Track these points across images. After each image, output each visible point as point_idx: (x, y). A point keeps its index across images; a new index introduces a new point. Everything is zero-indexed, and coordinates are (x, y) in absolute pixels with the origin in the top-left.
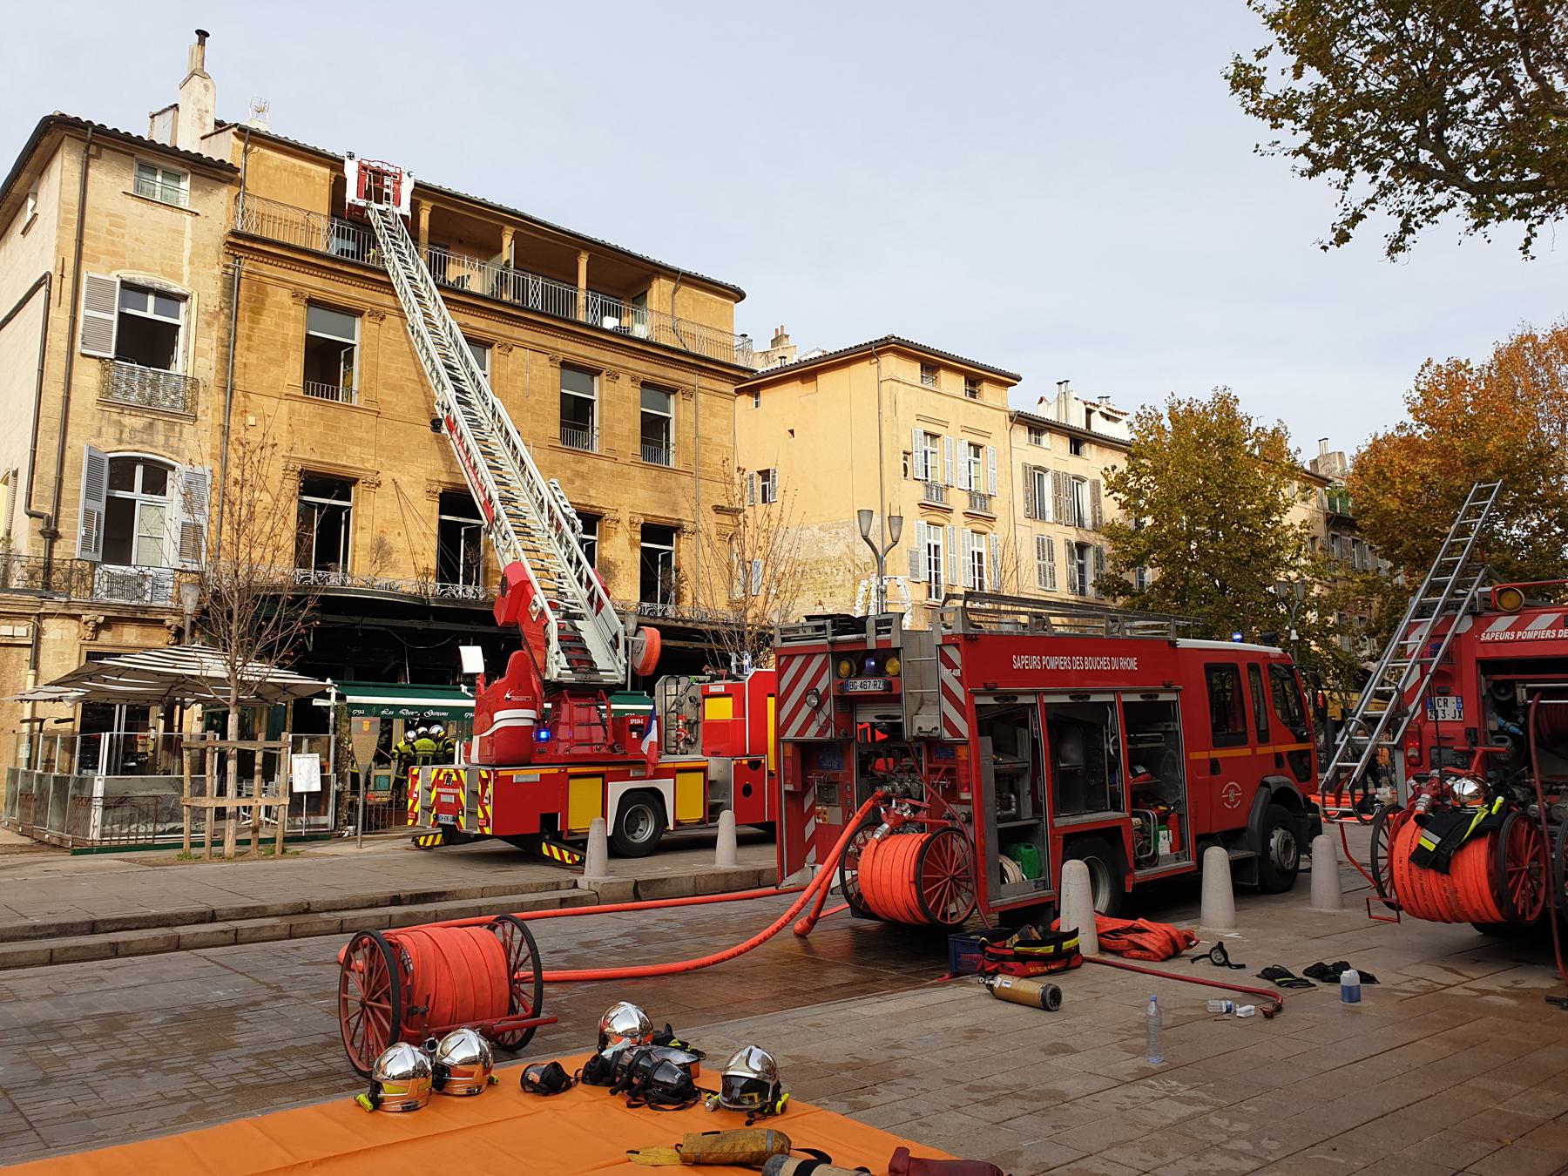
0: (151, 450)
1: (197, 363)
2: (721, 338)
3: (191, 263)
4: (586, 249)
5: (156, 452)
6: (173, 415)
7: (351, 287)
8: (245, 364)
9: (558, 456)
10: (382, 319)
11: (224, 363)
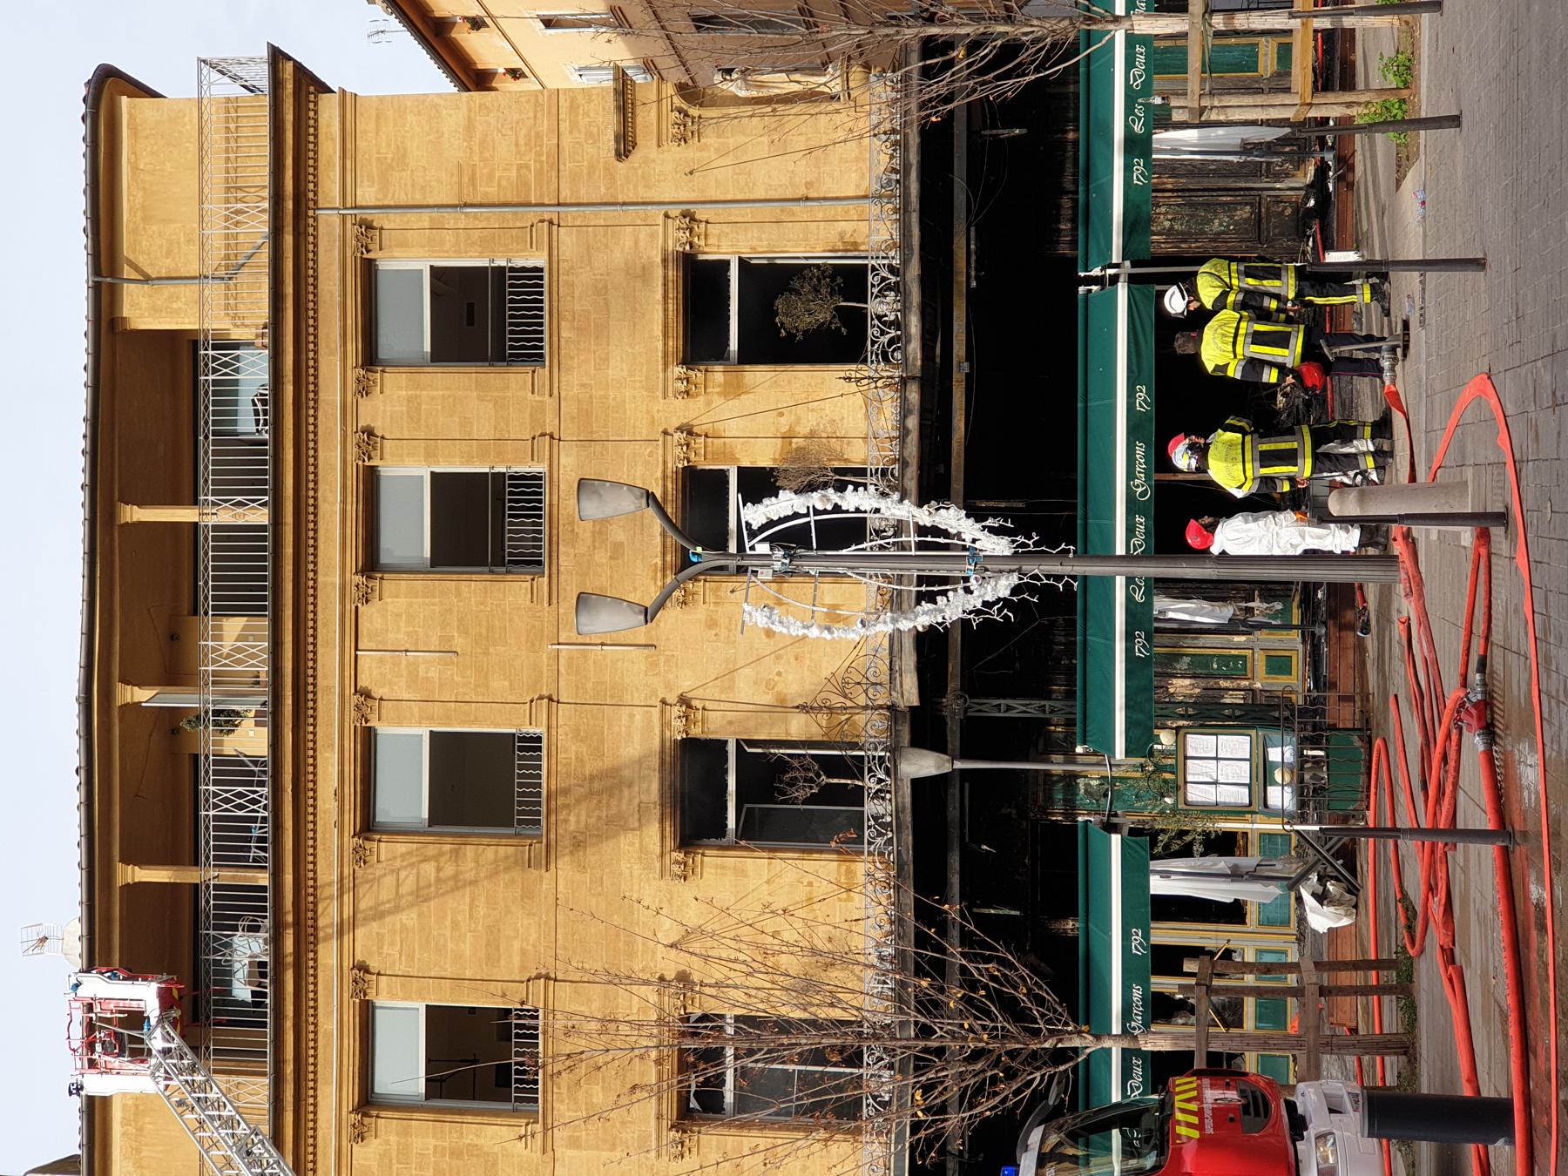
7: (321, 1030)
10: (367, 971)
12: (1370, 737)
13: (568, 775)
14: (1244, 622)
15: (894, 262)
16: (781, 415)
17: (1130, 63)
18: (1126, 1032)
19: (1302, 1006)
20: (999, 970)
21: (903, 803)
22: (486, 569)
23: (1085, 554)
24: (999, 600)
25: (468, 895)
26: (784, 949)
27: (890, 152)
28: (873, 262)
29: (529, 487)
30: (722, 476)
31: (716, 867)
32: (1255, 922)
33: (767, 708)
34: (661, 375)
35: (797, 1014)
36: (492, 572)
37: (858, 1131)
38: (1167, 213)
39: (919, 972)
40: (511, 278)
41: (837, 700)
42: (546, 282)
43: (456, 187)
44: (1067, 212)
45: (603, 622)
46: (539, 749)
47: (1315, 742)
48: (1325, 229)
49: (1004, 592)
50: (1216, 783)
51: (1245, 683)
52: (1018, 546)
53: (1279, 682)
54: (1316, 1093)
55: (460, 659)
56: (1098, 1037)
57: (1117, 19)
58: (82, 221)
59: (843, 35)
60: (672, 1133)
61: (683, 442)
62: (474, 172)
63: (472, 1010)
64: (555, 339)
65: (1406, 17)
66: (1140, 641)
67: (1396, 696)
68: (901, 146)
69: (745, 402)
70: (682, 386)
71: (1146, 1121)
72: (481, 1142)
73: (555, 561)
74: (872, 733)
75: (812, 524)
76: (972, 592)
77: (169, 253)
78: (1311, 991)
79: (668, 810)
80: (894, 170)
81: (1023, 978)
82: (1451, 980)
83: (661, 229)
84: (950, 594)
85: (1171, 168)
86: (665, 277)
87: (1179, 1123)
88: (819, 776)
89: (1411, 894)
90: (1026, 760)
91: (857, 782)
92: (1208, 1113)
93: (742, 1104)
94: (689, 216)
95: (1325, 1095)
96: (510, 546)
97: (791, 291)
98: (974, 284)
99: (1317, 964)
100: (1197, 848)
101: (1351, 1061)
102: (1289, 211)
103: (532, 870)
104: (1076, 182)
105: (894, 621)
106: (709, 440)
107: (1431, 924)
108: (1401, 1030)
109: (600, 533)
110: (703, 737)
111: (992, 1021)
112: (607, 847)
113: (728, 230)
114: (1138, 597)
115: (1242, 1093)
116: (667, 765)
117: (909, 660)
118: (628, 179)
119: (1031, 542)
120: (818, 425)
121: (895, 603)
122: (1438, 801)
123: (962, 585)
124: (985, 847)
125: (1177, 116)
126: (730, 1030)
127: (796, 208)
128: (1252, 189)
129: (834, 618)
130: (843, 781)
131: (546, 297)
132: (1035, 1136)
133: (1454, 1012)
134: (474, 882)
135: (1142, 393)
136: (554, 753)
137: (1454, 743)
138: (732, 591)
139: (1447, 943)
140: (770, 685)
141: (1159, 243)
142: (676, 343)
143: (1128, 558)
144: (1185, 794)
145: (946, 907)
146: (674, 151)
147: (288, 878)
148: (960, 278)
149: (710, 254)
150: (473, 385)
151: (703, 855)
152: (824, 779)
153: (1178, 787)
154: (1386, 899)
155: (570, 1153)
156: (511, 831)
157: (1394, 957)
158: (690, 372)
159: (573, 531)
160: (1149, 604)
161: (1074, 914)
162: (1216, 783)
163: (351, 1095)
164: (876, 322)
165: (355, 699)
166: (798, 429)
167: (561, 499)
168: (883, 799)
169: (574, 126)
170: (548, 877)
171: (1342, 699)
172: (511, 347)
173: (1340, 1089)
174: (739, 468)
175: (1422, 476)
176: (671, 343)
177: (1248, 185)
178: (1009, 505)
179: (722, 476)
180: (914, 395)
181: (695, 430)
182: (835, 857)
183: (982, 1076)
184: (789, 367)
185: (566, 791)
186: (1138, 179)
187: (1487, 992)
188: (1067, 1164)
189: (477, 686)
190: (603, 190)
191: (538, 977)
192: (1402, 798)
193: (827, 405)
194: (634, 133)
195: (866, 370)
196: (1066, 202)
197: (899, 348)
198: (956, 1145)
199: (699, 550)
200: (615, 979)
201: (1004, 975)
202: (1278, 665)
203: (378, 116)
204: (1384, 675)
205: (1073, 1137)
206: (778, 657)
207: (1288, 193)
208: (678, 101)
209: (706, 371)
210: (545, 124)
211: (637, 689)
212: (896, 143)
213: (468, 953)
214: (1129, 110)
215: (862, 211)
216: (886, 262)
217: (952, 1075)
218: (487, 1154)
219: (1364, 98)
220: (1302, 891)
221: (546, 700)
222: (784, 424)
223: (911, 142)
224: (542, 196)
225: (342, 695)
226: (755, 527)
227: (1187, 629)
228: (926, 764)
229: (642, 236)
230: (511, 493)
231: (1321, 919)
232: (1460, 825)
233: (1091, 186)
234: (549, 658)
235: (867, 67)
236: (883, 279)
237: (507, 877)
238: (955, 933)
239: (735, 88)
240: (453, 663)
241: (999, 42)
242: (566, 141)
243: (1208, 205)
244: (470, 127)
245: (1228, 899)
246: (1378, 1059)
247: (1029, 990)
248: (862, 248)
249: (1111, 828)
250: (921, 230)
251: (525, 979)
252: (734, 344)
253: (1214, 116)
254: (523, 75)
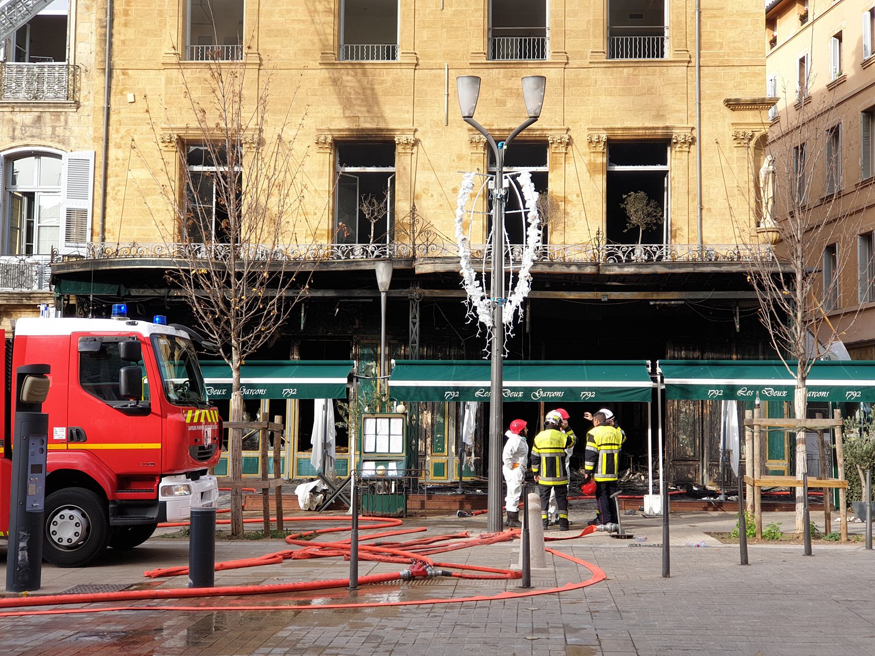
0: (39, 142)
1: (78, 50)
5: (43, 143)
6: (56, 105)
8: (123, 42)
11: (103, 46)
12: (402, 517)
13: (374, 75)
14: (463, 450)
15: (664, 258)
16: (578, 196)
17: (777, 388)
18: (241, 386)
19: (257, 480)
20: (273, 315)
21: (361, 265)
22: (490, 26)
23: (503, 365)
24: (478, 316)
25: (306, 18)
26: (282, 197)
27: (728, 255)
28: (664, 247)
29: (540, 52)
30: (543, 163)
31: (324, 161)
32: (299, 457)
33: (413, 189)
34: (601, 127)
35: (244, 209)
36: (489, 30)
37: (182, 239)
38: (690, 409)
39: (271, 274)
40: (658, 39)
41: (418, 228)
42: (655, 59)
43: (710, 7)
44: (691, 355)
45: (464, 91)
46: (388, 59)
47: (399, 487)
48: (681, 495)
49: (481, 319)
50: (376, 434)
51: (429, 451)
52: (507, 326)
53: (430, 467)
54: (211, 486)
55: (439, 12)
56: (238, 369)
57: (804, 379)
59: (796, 227)
60: (176, 137)
61: (563, 140)
62: (719, 17)
63: (241, 23)
64: (623, 65)
65: (801, 537)
66: (454, 394)
67: (426, 530)
68: (731, 262)
69: (585, 175)
70: (595, 139)
71: (193, 395)
72: (168, 27)
73: (495, 66)
74: (400, 248)
75: (519, 211)
76: (481, 300)
78: (265, 485)
79: (355, 133)
80: (717, 258)
81: (269, 328)
82: (275, 557)
83: (685, 125)
84: (481, 288)
85: (716, 412)
86: (658, 128)
87: (194, 412)
88: (375, 218)
89: (318, 538)
90: (386, 333)
91: (372, 240)
92: (199, 428)
93: (195, 175)
94: (693, 142)
95: (210, 491)
96: (503, 40)
97: (649, 200)
98: (652, 303)
99: (280, 487)
100: (340, 425)
101: (228, 507)
102: (690, 476)
103: (320, 55)
104: (708, 359)
105: (466, 257)
106: (564, 155)
107: (304, 548)
108: (245, 532)
109: (511, 93)
110: (396, 153)
111: (246, 312)
112: (334, 98)
113: (684, 164)
114: (478, 394)
115: (210, 446)
116: (380, 133)
117: (440, 268)
118: (715, 108)
119: (510, 333)
120: (572, 217)
121: (474, 260)
122: (370, 551)
123: (485, 294)
124: (337, 310)
125: (748, 413)
126: (236, 169)
127: (697, 203)
128: (703, 457)
129: (465, 226)
130: (372, 232)
131: (647, 59)
132: (184, 334)
133: (257, 558)
134: (313, 21)
135: (590, 395)
136: (386, 67)
137: (403, 559)
138: (478, 169)
139: (294, 555)
140: (426, 191)
141: (673, 405)
142: (619, 135)
143: (501, 388)
144: (370, 418)
145: (307, 286)
146: (730, 132)
148: (655, 296)
150: (596, 18)
151: (330, 153)
152: (373, 222)
153: (373, 414)
154: (315, 525)
155: (163, 78)
156: (342, 42)
157: (285, 529)
158: (603, 143)
159: (512, 77)
160: (474, 399)
161: (302, 357)
162: (376, 434)
164: (630, 249)
166: (570, 205)
167: (531, 68)
168: (363, 254)
170: (316, 64)
171: (423, 503)
172: (618, 40)
173: (214, 498)
174: (547, 173)
175: (548, 544)
176: (619, 132)
177: (705, 451)
178: (528, 323)
179: (543, 163)
180: (589, 270)
181: (570, 147)
182: (330, 227)
183: (215, 306)
184: (605, 200)
185: (365, 74)
186: (711, 393)
187: (270, 575)
188: (169, 351)
189: (424, 22)
190: (708, 92)
191: (261, 59)
192: (371, 533)
193: (584, 222)
194: (740, 110)
195: (603, 243)
196: (697, 354)
197: (615, 261)
198: (176, 293)
199: (505, 147)
200: (262, 101)
201: (270, 319)
202: (439, 469)
204: (437, 524)
205: (184, 357)
206: (441, 195)
207: (701, 476)
209: (603, 153)
210: (746, 59)
211: (423, 115)
212: (732, 259)
213: (274, 19)
214: (750, 387)
215: (694, 240)
216: (664, 254)
217: (215, 292)
218: (161, 31)
219: (756, 514)
220: (318, 481)
221: (416, 62)
222: (572, 197)
223: (733, 267)
224: (705, 56)
226: (518, 179)
227: (458, 421)
228: (383, 277)
229: (681, 114)
230: (534, 40)
231: (303, 492)
232: (360, 563)
233: (707, 367)
234: (440, 63)
235: (776, 242)
236: (655, 253)
237: (316, 41)
238: (291, 294)
239: (766, 166)
240: (437, 7)
241: (791, 314)
243: (694, 433)
244: (746, 14)
245: (312, 442)
246: (230, 521)
247: (263, 332)
248: (673, 240)
249: (351, 378)
250: (683, 273)
251: (260, 52)
252: (618, 168)
253: (748, 433)
254: (772, 47)
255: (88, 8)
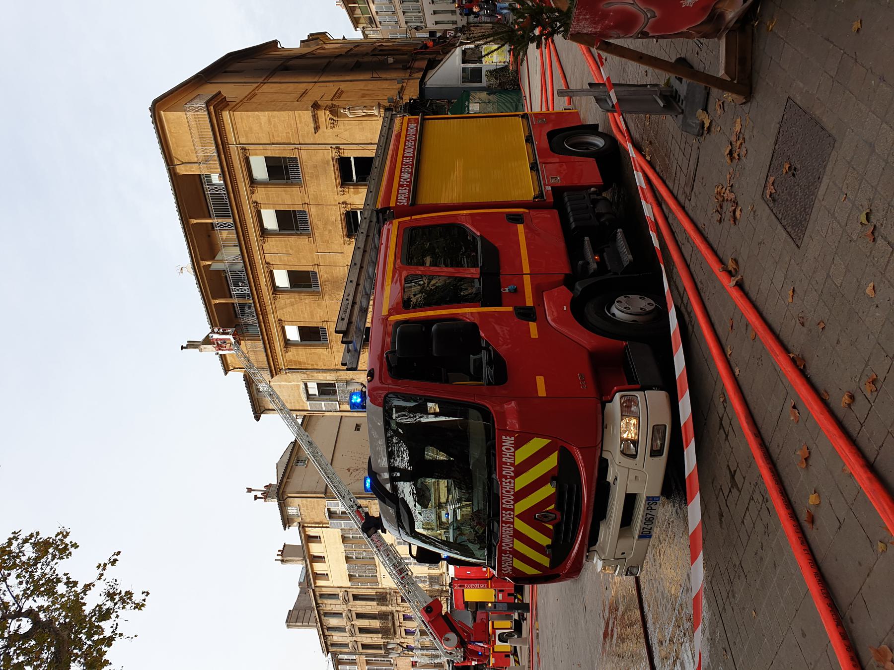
2: (193, 123)
3: (290, 382)
4: (188, 222)
9: (318, 239)
58: (160, 151)
77: (187, 156)
86: (333, 164)
142: (339, 181)
147: (258, 305)
149: (346, 154)
163: (283, 344)
165: (266, 265)
169: (301, 122)
203: (241, 118)
208: (331, 116)
225: (262, 264)
242: (299, 126)
244: (269, 121)
255: (312, 376)
